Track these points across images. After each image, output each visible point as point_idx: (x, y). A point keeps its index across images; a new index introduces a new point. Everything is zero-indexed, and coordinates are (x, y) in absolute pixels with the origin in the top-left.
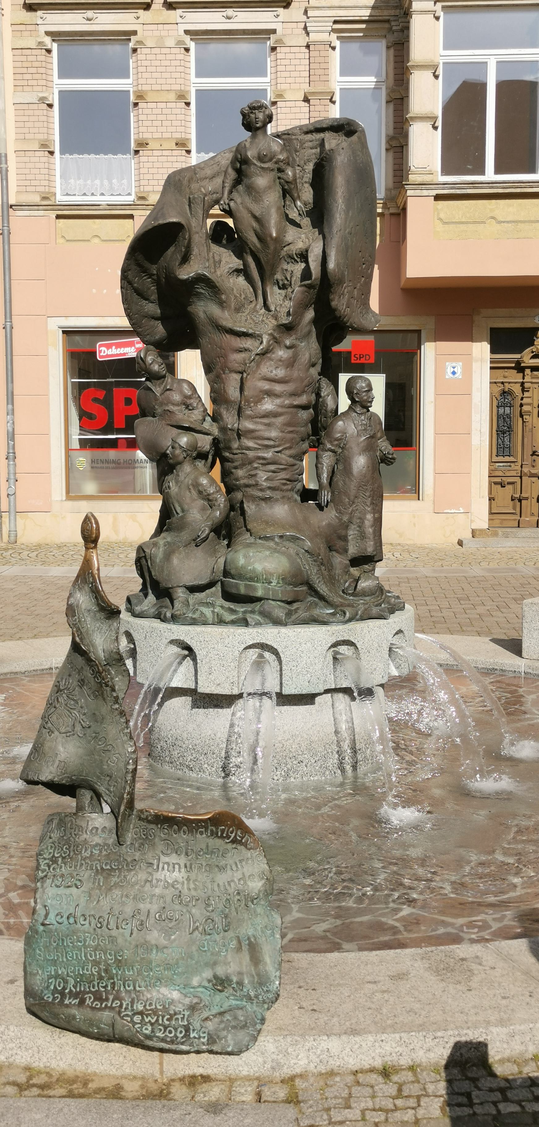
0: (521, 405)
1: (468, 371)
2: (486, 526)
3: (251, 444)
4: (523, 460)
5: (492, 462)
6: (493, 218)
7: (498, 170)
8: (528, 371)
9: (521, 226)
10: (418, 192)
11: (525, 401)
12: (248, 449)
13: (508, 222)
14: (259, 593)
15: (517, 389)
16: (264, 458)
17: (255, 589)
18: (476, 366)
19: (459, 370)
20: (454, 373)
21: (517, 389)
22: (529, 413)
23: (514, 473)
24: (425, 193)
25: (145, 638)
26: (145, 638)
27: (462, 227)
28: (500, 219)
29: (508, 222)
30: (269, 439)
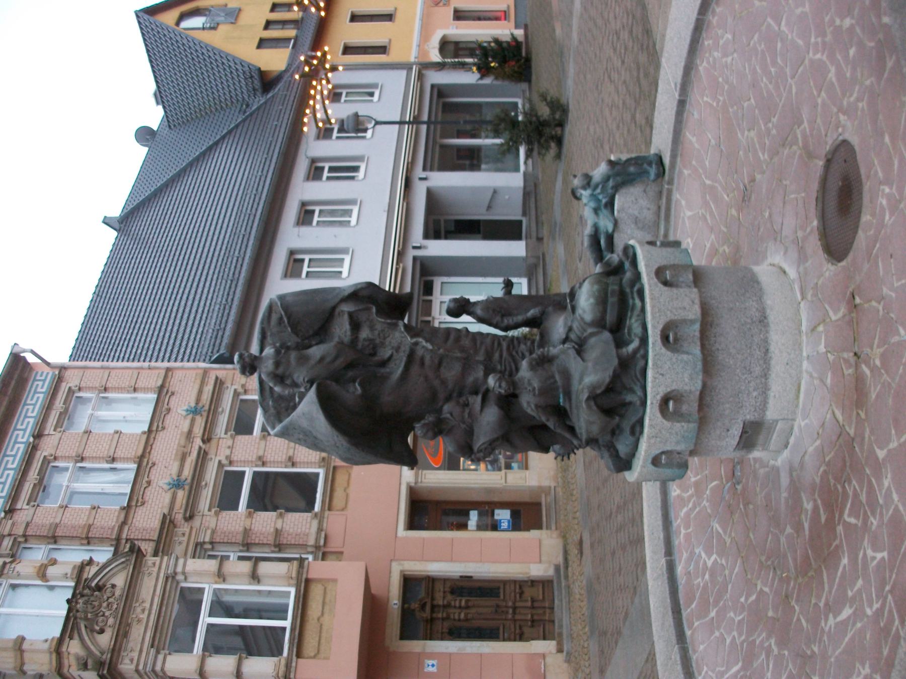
0: (459, 620)
1: (431, 656)
2: (554, 643)
3: (497, 356)
4: (502, 619)
5: (504, 640)
6: (318, 619)
7: (285, 619)
8: (435, 615)
9: (327, 600)
10: (293, 669)
11: (456, 617)
12: (501, 356)
13: (323, 608)
14: (616, 288)
15: (446, 624)
16: (508, 348)
17: (613, 291)
18: (428, 650)
19: (430, 662)
20: (433, 665)
21: (446, 624)
22: (466, 615)
23: (512, 626)
24: (294, 664)
25: (662, 375)
26: (662, 375)
27: (323, 641)
28: (320, 614)
29: (323, 608)
30: (493, 343)
